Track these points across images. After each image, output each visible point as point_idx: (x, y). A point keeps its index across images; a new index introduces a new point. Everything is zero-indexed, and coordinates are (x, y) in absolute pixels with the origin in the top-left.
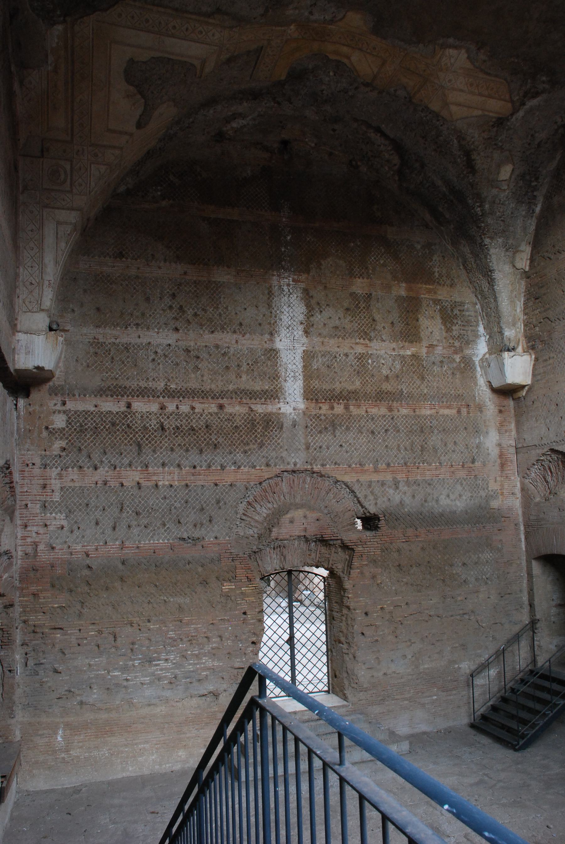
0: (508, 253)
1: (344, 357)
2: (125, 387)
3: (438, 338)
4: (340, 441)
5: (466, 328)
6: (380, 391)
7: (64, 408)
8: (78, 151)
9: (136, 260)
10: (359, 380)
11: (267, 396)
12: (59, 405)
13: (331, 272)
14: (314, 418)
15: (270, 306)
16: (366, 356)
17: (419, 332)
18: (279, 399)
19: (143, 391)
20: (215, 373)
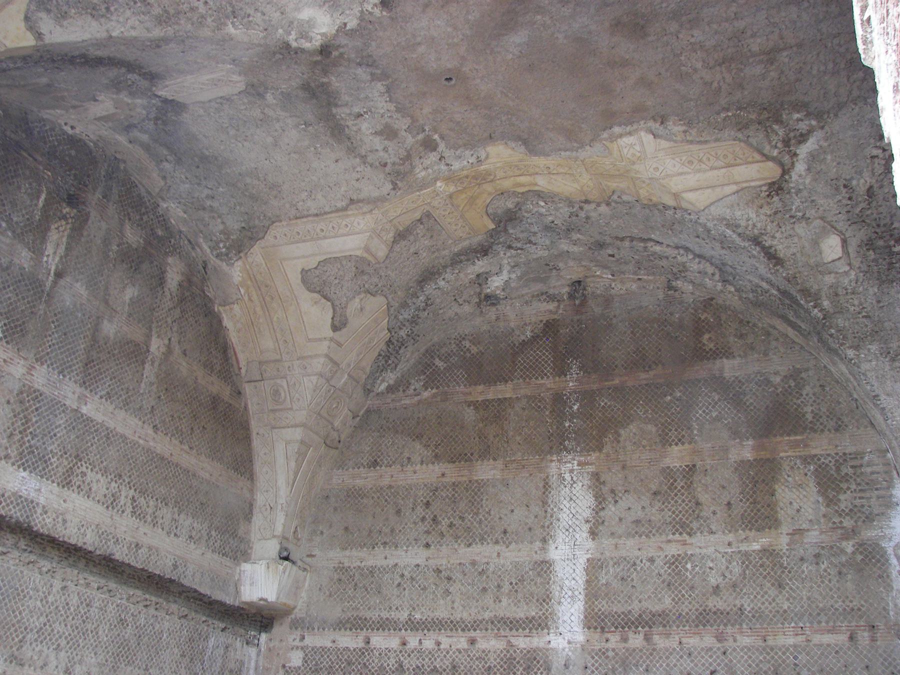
0: (897, 364)
1: (648, 564)
2: (366, 619)
3: (810, 517)
5: (868, 495)
6: (705, 611)
7: (301, 644)
9: (390, 466)
11: (534, 625)
12: (298, 640)
13: (635, 443)
14: (597, 654)
15: (545, 503)
16: (683, 558)
17: (777, 512)
18: (548, 629)
19: (384, 622)
20: (468, 598)
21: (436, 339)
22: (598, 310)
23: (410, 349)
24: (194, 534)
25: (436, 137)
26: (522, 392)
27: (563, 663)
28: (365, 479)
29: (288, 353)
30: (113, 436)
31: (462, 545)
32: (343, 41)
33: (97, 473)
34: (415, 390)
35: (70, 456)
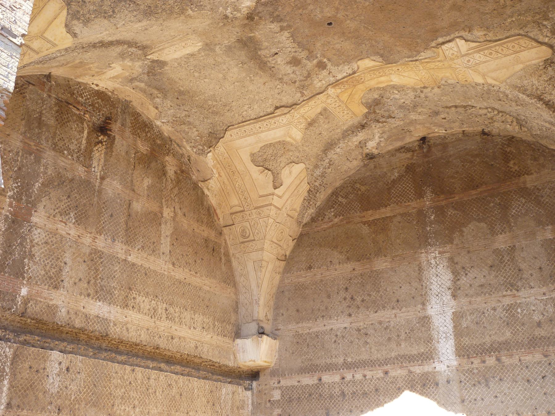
2: (317, 365)
4: (494, 392)
7: (279, 385)
9: (320, 268)
10: (509, 331)
11: (424, 358)
12: (276, 383)
13: (474, 236)
14: (466, 372)
16: (515, 306)
18: (433, 359)
19: (329, 366)
22: (439, 154)
25: (325, 60)
26: (397, 211)
27: (446, 380)
28: (305, 277)
30: (149, 272)
31: (372, 312)
32: (260, 9)
33: (142, 296)
35: (125, 288)
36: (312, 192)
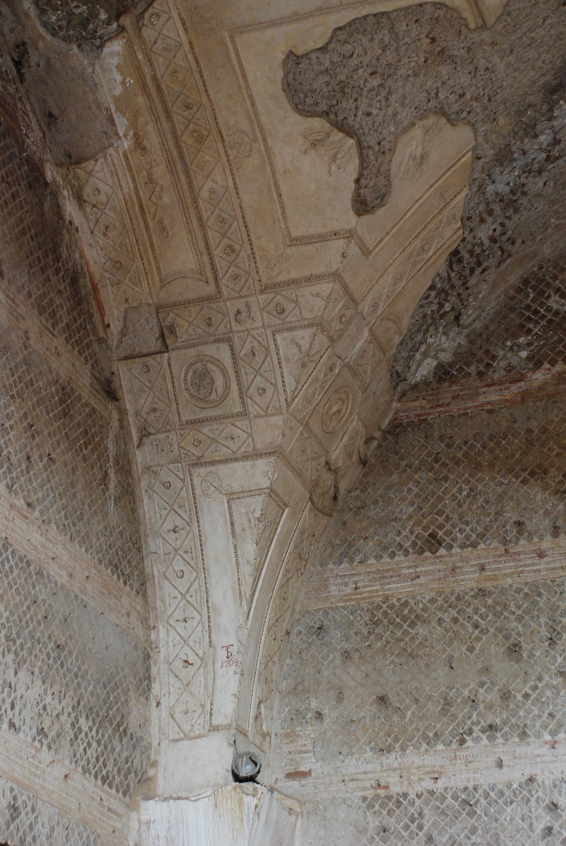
8: (238, 312)
9: (474, 545)
21: (547, 250)
23: (491, 275)
24: (47, 724)
29: (236, 278)
34: (510, 369)
36: (462, 263)
